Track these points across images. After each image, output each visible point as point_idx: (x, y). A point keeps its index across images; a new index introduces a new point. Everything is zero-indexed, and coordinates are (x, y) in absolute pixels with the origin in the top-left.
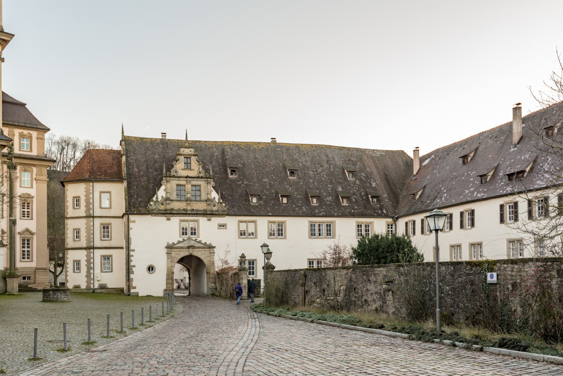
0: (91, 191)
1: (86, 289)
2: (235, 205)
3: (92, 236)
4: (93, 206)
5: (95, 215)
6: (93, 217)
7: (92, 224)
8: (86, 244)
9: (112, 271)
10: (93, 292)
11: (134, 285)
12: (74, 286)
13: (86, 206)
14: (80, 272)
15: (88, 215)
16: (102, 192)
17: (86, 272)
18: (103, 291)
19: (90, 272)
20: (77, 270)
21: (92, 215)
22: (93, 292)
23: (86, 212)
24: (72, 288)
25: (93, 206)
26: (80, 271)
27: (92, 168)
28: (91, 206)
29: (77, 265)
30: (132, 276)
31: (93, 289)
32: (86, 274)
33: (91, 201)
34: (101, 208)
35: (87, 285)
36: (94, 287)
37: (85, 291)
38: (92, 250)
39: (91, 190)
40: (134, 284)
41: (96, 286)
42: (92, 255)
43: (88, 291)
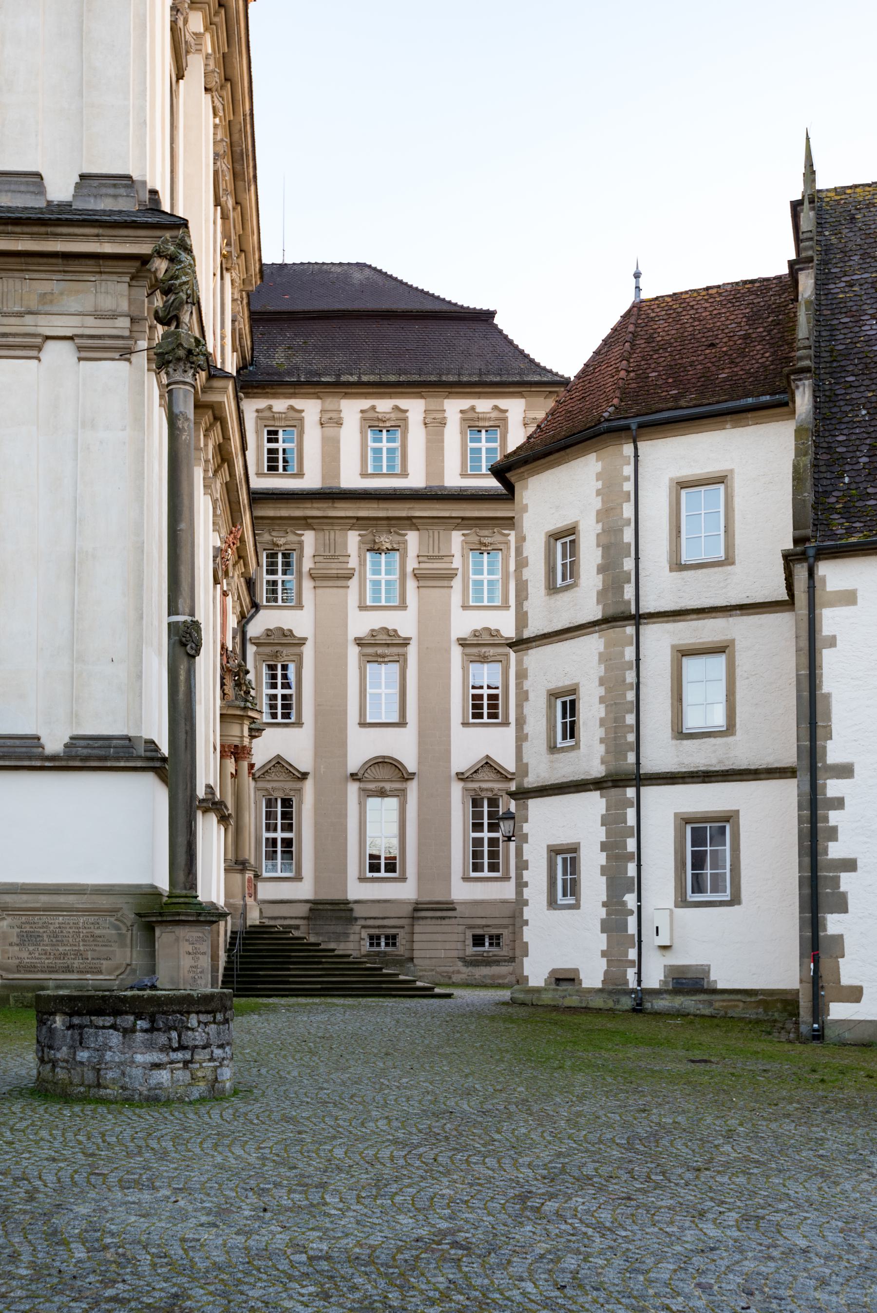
0: (629, 486)
1: (600, 991)
3: (630, 719)
4: (637, 559)
5: (648, 605)
6: (639, 619)
7: (629, 653)
8: (603, 762)
9: (735, 900)
10: (638, 1009)
11: (846, 980)
12: (554, 971)
13: (602, 569)
14: (576, 906)
15: (611, 611)
16: (683, 485)
17: (604, 905)
18: (688, 1003)
19: (624, 904)
20: (565, 894)
21: (633, 611)
22: (634, 1010)
23: (602, 595)
24: (542, 984)
25: (637, 559)
26: (578, 900)
27: (642, 377)
28: (629, 564)
29: (565, 873)
30: (833, 924)
31: (633, 991)
32: (603, 913)
33: (628, 536)
34: (678, 566)
35: (606, 973)
36: (639, 982)
37: (598, 1002)
38: (631, 792)
39: (627, 479)
40: (848, 974)
42: (631, 813)
43: (610, 1004)
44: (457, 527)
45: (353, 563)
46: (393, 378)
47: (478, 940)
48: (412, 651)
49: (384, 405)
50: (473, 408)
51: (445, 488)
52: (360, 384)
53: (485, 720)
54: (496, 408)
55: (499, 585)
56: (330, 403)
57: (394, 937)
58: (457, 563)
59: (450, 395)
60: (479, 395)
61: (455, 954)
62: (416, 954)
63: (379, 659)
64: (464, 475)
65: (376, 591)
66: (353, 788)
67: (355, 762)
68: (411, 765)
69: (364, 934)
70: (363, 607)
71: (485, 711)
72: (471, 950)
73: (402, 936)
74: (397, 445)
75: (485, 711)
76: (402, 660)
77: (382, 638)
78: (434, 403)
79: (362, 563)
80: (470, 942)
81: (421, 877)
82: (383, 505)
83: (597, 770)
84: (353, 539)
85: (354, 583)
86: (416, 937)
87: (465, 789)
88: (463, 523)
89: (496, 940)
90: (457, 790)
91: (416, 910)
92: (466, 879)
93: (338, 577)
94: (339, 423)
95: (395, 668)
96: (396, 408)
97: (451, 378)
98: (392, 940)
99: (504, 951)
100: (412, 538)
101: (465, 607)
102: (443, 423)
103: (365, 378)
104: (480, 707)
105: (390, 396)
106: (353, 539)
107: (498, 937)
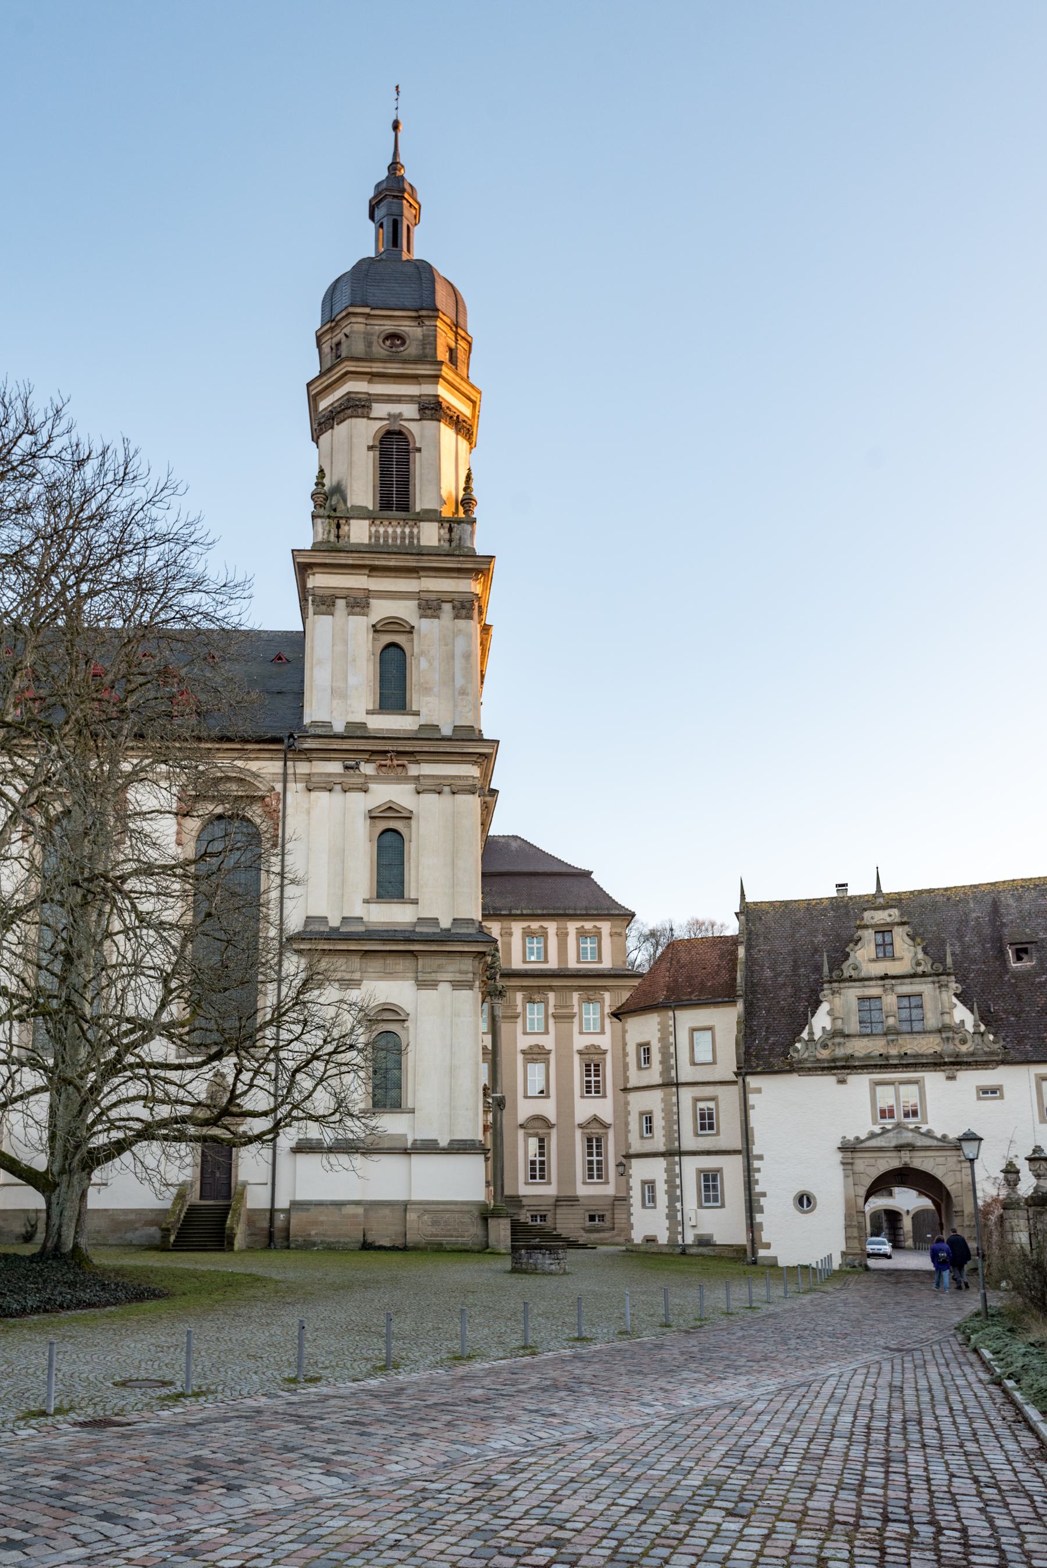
2: (1025, 1037)
41: (690, 1239)
44: (576, 990)
45: (519, 1009)
46: (539, 912)
47: (592, 1218)
48: (552, 1058)
49: (535, 925)
50: (583, 927)
51: (568, 969)
52: (522, 915)
53: (593, 1094)
54: (595, 927)
55: (599, 1021)
56: (506, 924)
57: (545, 1216)
58: (576, 1010)
59: (570, 920)
60: (586, 920)
61: (580, 1226)
62: (558, 1226)
63: (534, 1061)
64: (579, 962)
65: (532, 1024)
66: (521, 1133)
67: (522, 1118)
68: (553, 1119)
69: (529, 1214)
70: (525, 1033)
71: (593, 1089)
72: (588, 1224)
73: (550, 1215)
74: (542, 945)
75: (593, 1089)
76: (547, 1062)
77: (536, 1050)
78: (561, 924)
79: (524, 1009)
80: (587, 1219)
81: (560, 1183)
82: (537, 980)
83: (662, 1148)
84: (519, 996)
85: (520, 1020)
86: (558, 1216)
87: (583, 1133)
88: (579, 988)
89: (602, 1218)
90: (578, 1134)
91: (557, 1201)
92: (584, 1183)
93: (512, 1017)
94: (511, 934)
95: (543, 1065)
96: (541, 927)
97: (571, 912)
98: (543, 1218)
99: (607, 1224)
100: (551, 996)
101: (581, 1033)
102: (567, 934)
103: (525, 912)
104: (590, 1087)
105: (538, 920)
106: (519, 996)
107: (603, 1216)
